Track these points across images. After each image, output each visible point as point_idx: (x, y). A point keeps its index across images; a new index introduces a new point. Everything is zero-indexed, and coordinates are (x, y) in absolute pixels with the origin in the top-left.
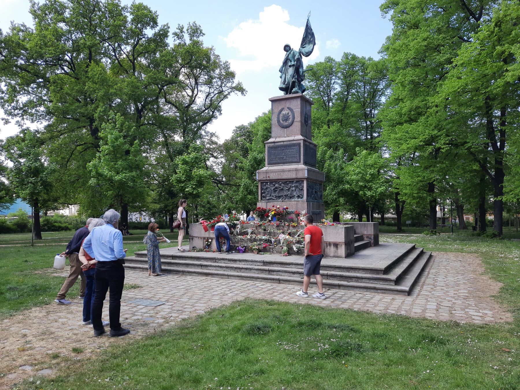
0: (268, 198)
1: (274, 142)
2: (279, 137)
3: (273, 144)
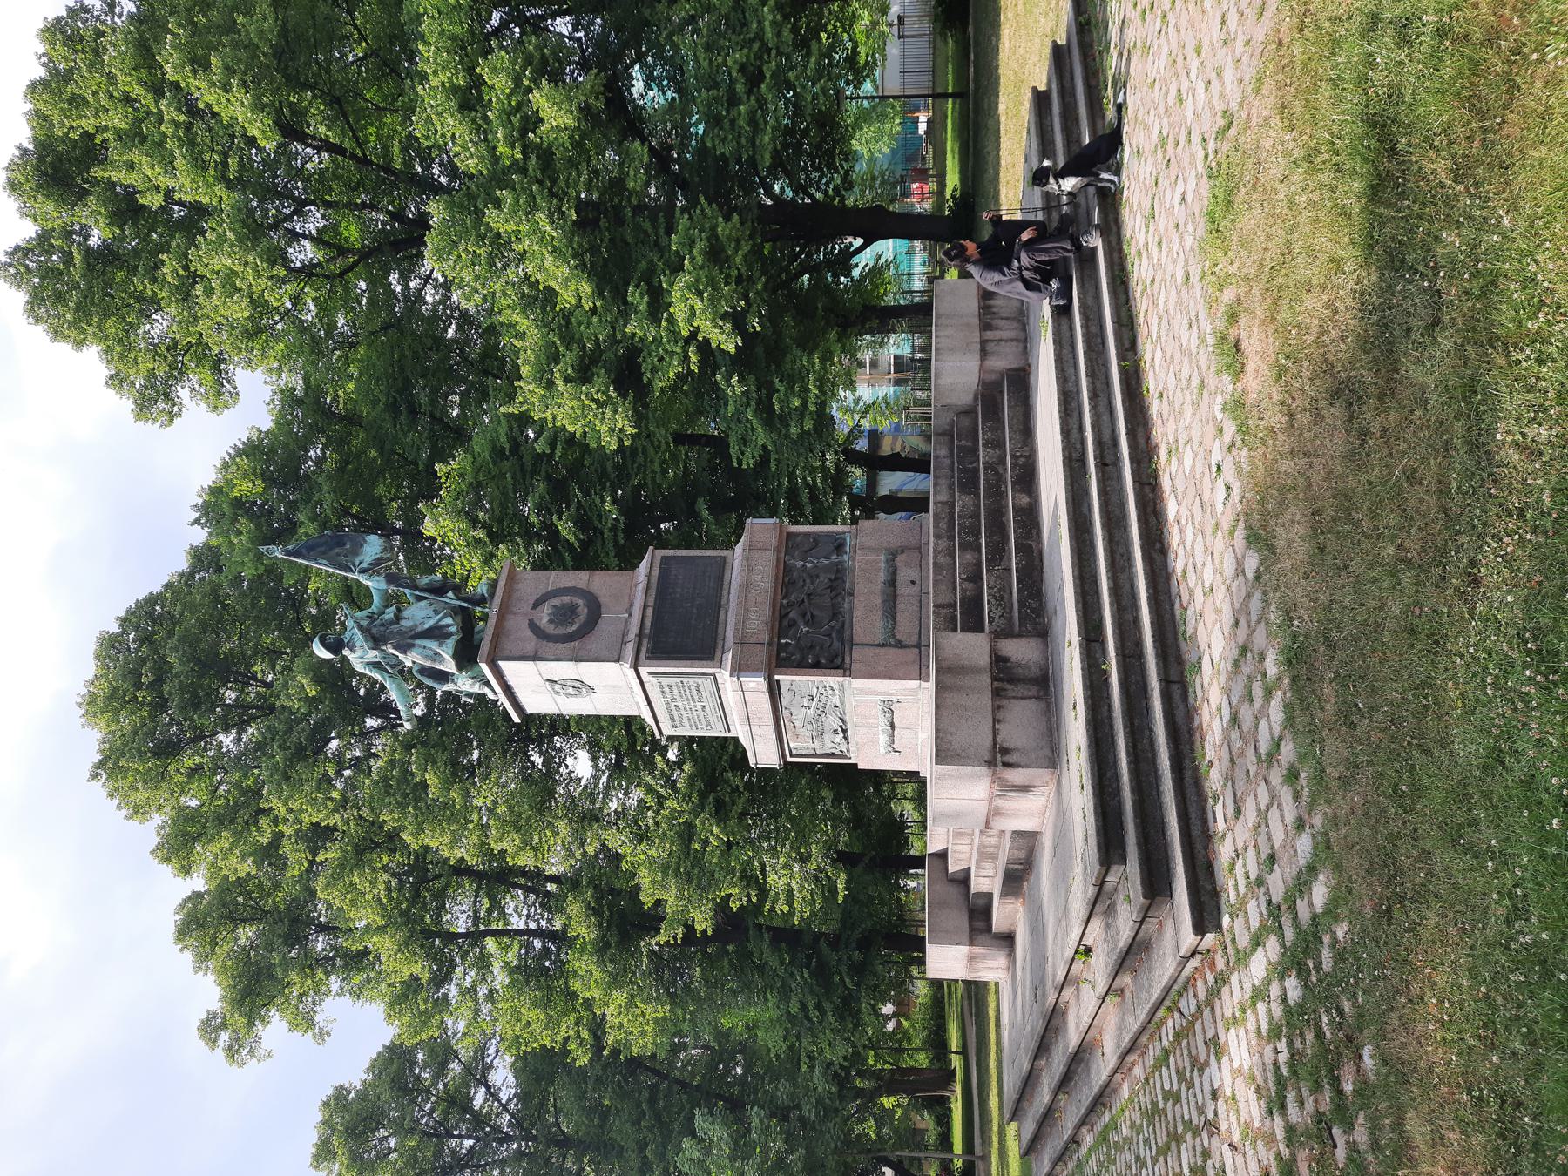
0: (836, 644)
1: (640, 636)
2: (625, 634)
3: (645, 641)
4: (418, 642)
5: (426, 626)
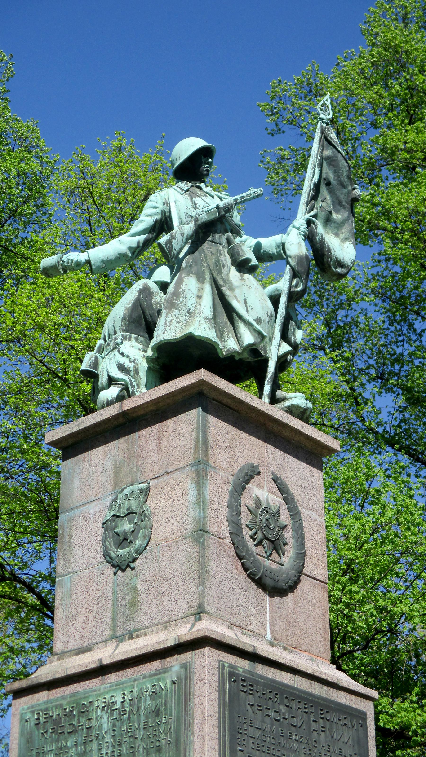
3: (242, 665)
4: (208, 288)
5: (235, 304)
